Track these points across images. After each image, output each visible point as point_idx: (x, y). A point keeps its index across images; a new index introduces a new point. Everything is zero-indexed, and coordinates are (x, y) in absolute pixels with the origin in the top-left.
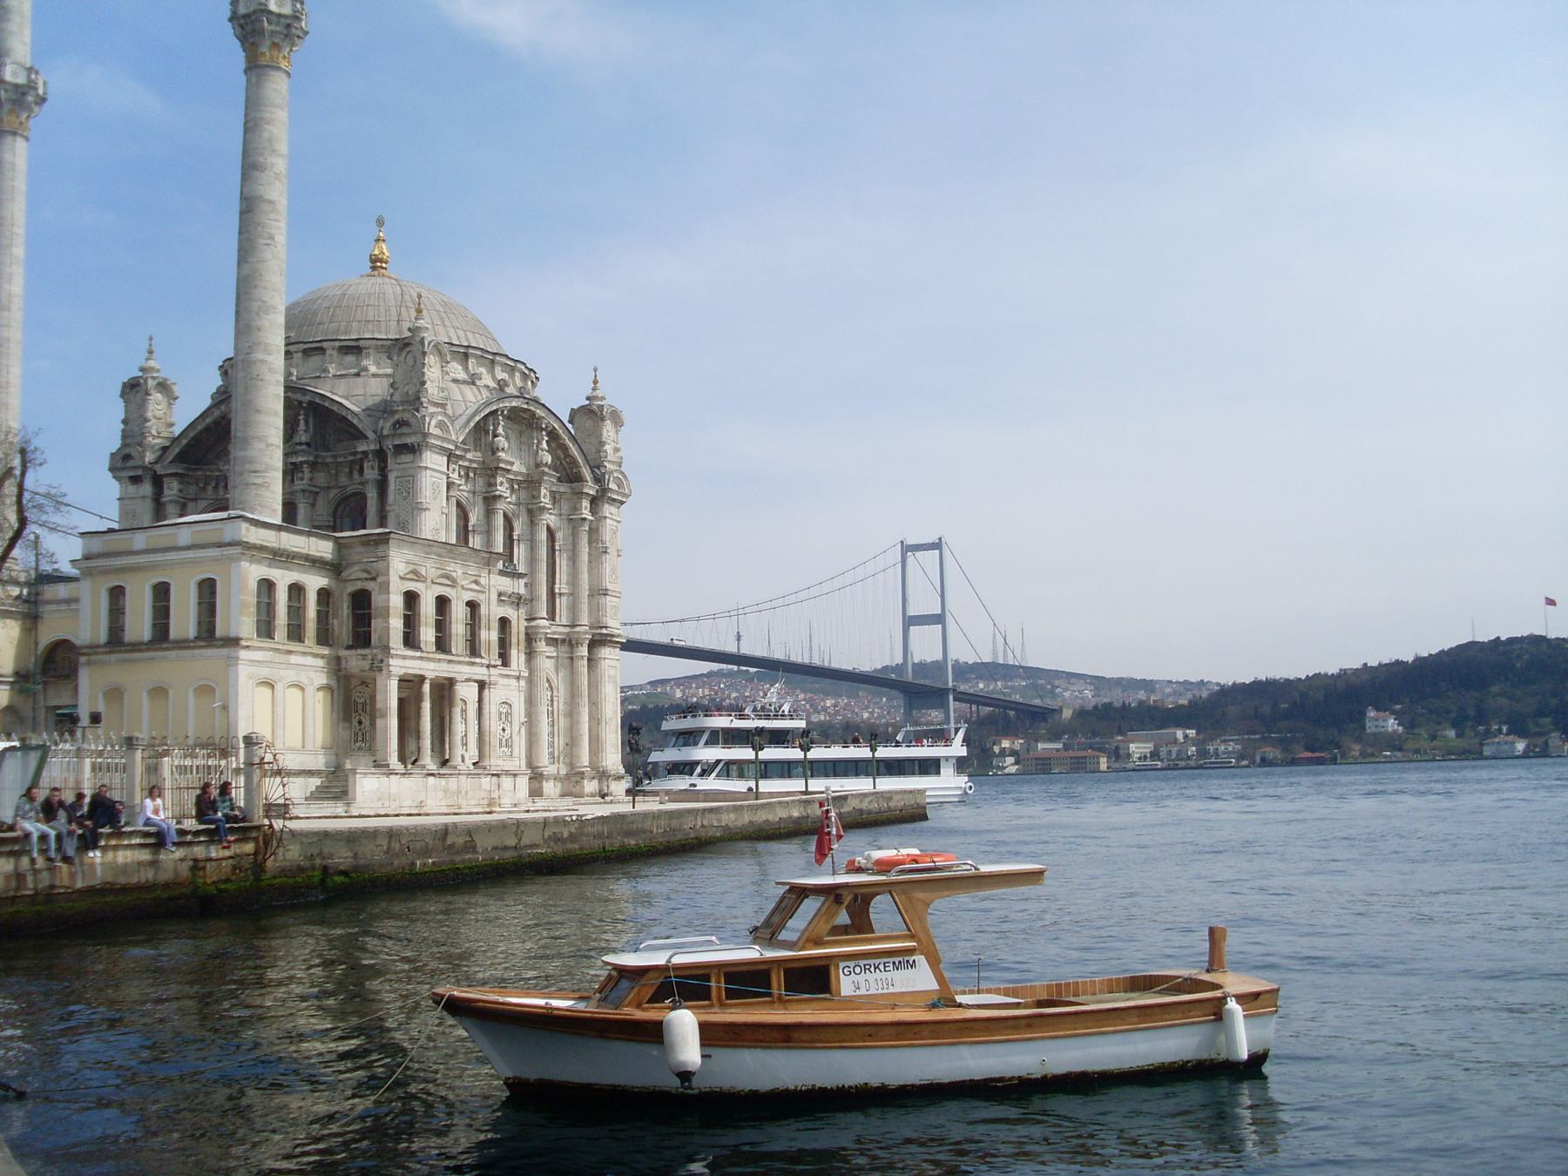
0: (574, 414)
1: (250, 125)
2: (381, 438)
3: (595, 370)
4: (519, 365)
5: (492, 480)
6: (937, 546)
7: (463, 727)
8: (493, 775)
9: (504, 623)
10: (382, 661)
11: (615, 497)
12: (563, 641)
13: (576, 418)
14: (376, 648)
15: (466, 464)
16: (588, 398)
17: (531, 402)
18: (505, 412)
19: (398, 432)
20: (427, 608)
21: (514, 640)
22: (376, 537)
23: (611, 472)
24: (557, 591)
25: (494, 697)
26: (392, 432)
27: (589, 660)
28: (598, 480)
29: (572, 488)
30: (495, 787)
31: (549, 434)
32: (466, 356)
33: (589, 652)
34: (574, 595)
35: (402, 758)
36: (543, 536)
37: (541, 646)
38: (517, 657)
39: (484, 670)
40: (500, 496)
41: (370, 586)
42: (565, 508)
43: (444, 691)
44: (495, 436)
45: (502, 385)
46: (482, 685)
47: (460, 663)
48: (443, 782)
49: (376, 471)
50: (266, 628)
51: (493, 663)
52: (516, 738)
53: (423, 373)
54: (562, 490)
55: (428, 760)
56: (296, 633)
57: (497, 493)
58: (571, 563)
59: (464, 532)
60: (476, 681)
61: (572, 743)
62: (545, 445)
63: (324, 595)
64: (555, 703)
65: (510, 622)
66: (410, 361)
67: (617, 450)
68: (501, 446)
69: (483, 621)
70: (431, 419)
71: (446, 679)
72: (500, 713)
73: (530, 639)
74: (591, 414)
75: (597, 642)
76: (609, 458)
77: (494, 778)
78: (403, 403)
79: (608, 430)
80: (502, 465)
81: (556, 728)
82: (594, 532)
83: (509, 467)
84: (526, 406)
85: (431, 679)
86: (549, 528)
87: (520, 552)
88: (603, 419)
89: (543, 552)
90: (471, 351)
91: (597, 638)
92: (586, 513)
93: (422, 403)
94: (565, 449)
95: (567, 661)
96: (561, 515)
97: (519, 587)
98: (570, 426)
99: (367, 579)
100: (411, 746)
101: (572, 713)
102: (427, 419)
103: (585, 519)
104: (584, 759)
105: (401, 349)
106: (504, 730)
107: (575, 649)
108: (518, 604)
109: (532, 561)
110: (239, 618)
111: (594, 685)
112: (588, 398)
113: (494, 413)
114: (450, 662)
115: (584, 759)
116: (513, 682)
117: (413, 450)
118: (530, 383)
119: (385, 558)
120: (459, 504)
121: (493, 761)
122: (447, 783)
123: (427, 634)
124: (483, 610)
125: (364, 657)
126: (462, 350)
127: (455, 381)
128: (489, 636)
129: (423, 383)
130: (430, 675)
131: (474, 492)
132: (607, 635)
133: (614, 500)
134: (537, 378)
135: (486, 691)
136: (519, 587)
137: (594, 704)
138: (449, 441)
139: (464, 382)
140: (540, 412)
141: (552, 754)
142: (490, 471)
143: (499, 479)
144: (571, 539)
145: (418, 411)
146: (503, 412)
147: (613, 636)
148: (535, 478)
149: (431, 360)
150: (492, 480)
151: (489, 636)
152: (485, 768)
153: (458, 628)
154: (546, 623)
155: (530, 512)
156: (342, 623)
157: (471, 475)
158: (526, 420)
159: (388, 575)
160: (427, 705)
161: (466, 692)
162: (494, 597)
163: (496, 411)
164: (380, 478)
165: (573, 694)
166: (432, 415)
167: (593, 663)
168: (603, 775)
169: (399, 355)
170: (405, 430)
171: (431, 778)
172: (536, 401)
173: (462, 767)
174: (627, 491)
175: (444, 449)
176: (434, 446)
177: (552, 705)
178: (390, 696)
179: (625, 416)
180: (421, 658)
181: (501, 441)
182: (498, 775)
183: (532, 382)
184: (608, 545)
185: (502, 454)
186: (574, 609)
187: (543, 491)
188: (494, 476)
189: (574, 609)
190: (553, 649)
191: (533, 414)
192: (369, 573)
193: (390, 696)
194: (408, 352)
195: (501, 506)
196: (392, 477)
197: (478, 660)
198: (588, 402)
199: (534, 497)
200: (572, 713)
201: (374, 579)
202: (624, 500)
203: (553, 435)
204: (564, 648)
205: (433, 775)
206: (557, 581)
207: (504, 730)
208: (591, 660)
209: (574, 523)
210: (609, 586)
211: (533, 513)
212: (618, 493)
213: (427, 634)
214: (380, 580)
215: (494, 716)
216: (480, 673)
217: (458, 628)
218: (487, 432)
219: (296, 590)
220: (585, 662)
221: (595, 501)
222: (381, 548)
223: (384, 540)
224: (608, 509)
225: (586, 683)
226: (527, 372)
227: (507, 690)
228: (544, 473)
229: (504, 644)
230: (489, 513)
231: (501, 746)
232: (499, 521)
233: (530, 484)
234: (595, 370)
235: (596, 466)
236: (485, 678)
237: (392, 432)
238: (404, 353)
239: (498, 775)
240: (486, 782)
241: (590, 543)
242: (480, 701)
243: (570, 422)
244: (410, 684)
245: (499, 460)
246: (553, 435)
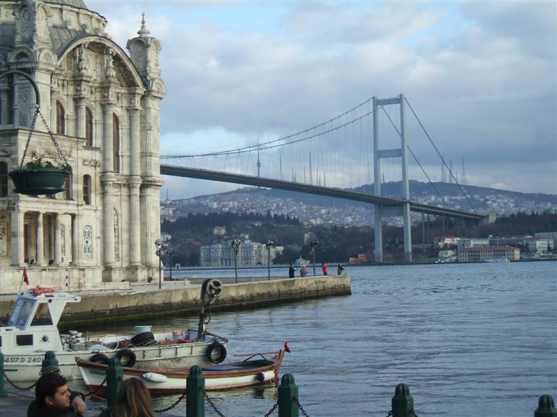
0: (130, 42)
2: (8, 65)
3: (143, 15)
4: (95, 15)
5: (79, 88)
6: (399, 100)
7: (63, 241)
8: (80, 269)
9: (87, 178)
10: (14, 204)
11: (156, 95)
12: (124, 185)
13: (131, 46)
14: (11, 196)
15: (62, 78)
16: (139, 33)
17: (103, 39)
18: (86, 45)
19: (21, 60)
21: (93, 188)
22: (9, 132)
23: (153, 80)
24: (120, 154)
25: (80, 224)
26: (16, 60)
27: (140, 196)
28: (146, 84)
29: (129, 90)
30: (82, 276)
31: (114, 58)
32: (61, 10)
33: (140, 192)
34: (131, 157)
35: (26, 261)
36: (111, 121)
37: (111, 190)
38: (95, 198)
39: (75, 207)
40: (84, 98)
41: (7, 160)
42: (125, 103)
43: (51, 219)
44: (80, 60)
45: (83, 27)
46: (73, 216)
47: (61, 203)
48: (50, 274)
49: (6, 84)
51: (80, 203)
52: (94, 246)
53: (35, 25)
54: (123, 91)
55: (43, 262)
57: (82, 96)
58: (129, 137)
59: (61, 119)
60: (70, 214)
61: (131, 247)
62: (111, 64)
64: (120, 224)
65: (90, 177)
66: (27, 17)
67: (157, 65)
68: (84, 66)
69: (74, 179)
70: (40, 52)
71: (52, 213)
72: (85, 232)
73: (103, 184)
74: (140, 43)
75: (143, 187)
76: (152, 71)
77: (81, 272)
78: (22, 42)
79: (151, 53)
80: (84, 78)
81: (120, 238)
82: (143, 117)
83: (89, 80)
84: (99, 41)
85: (43, 214)
86: (114, 115)
87: (97, 131)
88: (148, 46)
89: (111, 132)
90: (64, 7)
91: (145, 183)
92: (138, 105)
93: (34, 43)
94: (124, 66)
95: (126, 198)
96: (122, 107)
97: (97, 156)
98: (127, 51)
99: (5, 156)
100: (32, 253)
101: (130, 230)
102: (38, 53)
103: (137, 110)
104: (138, 258)
105: (21, 9)
106: (87, 242)
107: (132, 190)
108: (95, 166)
109: (104, 137)
111: (143, 212)
112: (139, 33)
113: (79, 46)
114: (54, 203)
115: (138, 258)
116: (93, 213)
117: (31, 71)
118: (101, 24)
119: (15, 144)
120: (58, 103)
121: (81, 261)
122: (53, 274)
125: (4, 202)
126: (60, 6)
127: (55, 27)
129: (34, 31)
130: (43, 211)
131: (68, 95)
132: (151, 181)
133: (155, 97)
134: (106, 22)
135: (76, 220)
136: (97, 156)
137: (144, 224)
138: (51, 65)
139: (61, 28)
140: (108, 44)
141: (117, 256)
142: (77, 80)
143: (83, 87)
144: (128, 122)
145: (32, 48)
146: (84, 45)
147: (155, 182)
148: (106, 85)
149: (40, 15)
150: (79, 88)
151: (78, 187)
152: (76, 266)
154: (113, 174)
155: (103, 106)
157: (66, 85)
158: (100, 48)
159: (17, 153)
160: (41, 229)
161: (65, 220)
162: (80, 163)
163: (81, 45)
164: (8, 88)
165: (131, 218)
166: (41, 50)
167: (143, 198)
168: (148, 267)
169: (20, 13)
170: (24, 59)
171: (44, 273)
172: (105, 37)
173: (62, 265)
174: (164, 91)
175: (48, 70)
176: (42, 69)
177: (118, 225)
178: (20, 222)
179: (163, 47)
180: (37, 202)
181: (84, 64)
182: (83, 270)
183: (103, 24)
184: (152, 125)
185: (84, 71)
186: (131, 165)
187: (110, 94)
188: (80, 85)
189: (131, 165)
190: (117, 190)
191: (104, 46)
192: (3, 151)
193: (20, 222)
194: (26, 10)
195: (84, 105)
196: (16, 88)
197: (71, 202)
198: (138, 36)
199: (104, 97)
200: (130, 230)
201: (9, 156)
202: (162, 97)
203: (117, 59)
204: (125, 191)
205: (45, 270)
206: (120, 148)
207: (87, 242)
208: (142, 197)
209: (131, 110)
210: (153, 151)
211: (105, 105)
212: (158, 92)
214: (13, 156)
215: (81, 234)
216: (72, 208)
218: (75, 58)
220: (138, 198)
221: (143, 98)
222: (13, 138)
223: (14, 133)
224: (152, 103)
225: (138, 211)
226: (100, 18)
227: (89, 217)
228: (110, 82)
229: (87, 191)
231: (85, 252)
232: (83, 113)
233: (104, 87)
234: (143, 15)
235: (144, 77)
236: (76, 212)
237: (16, 60)
238: (23, 11)
239: (83, 270)
240: (76, 273)
241: (142, 123)
242: (73, 225)
243: (128, 48)
244: (31, 216)
245: (82, 75)
246: (117, 59)
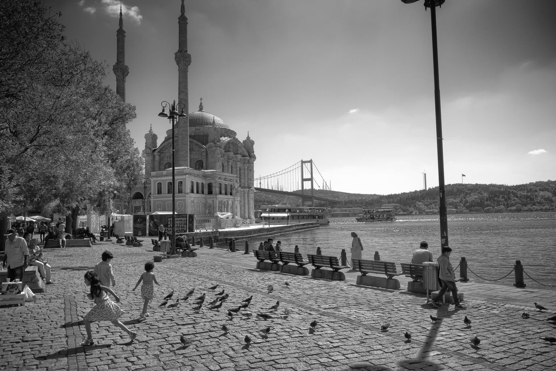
1: (180, 82)
6: (311, 161)
20: (223, 187)
50: (192, 191)
56: (198, 192)
61: (245, 212)
63: (202, 184)
110: (188, 189)
111: (248, 201)
123: (223, 192)
124: (233, 187)
128: (234, 192)
153: (229, 190)
156: (206, 190)
200: (244, 206)
213: (223, 192)
217: (229, 190)
219: (197, 183)
230: (228, 164)
